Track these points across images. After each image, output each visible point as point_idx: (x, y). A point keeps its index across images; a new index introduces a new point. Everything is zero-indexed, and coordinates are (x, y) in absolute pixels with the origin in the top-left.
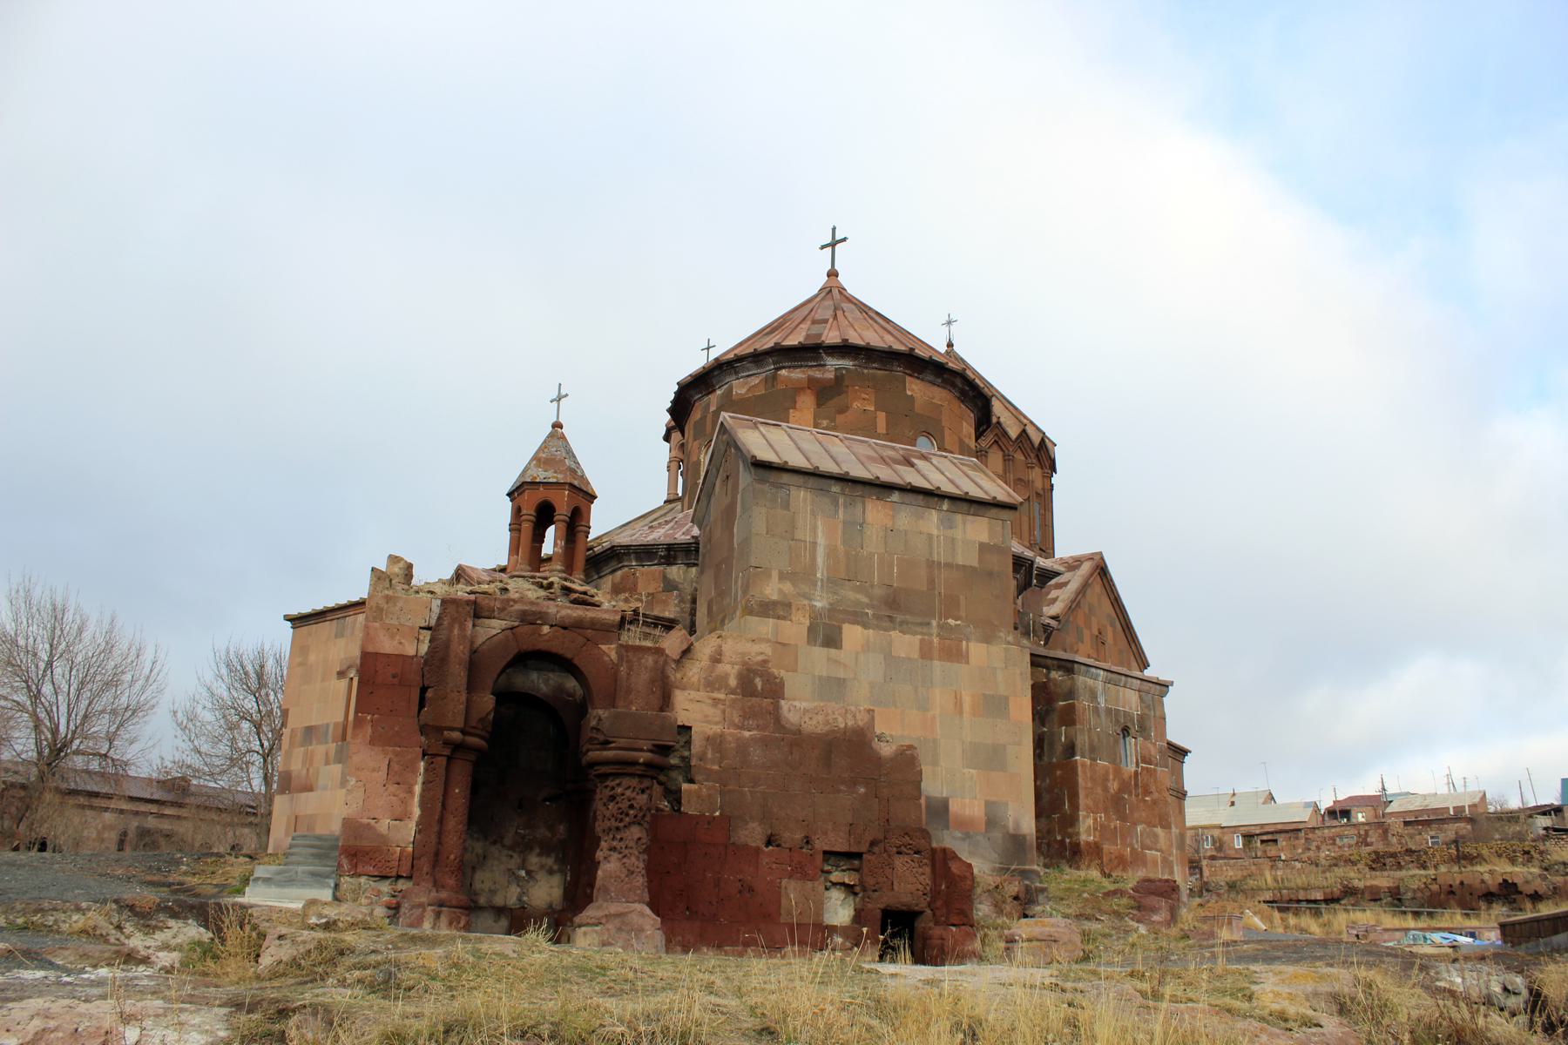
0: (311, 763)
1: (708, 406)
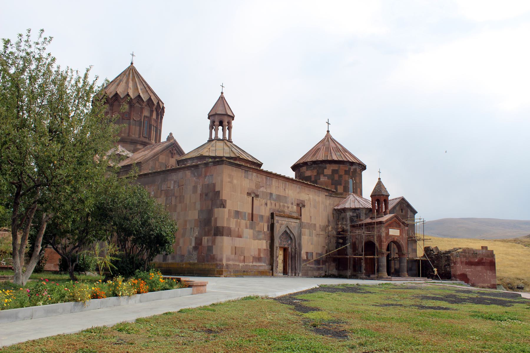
0: (240, 226)
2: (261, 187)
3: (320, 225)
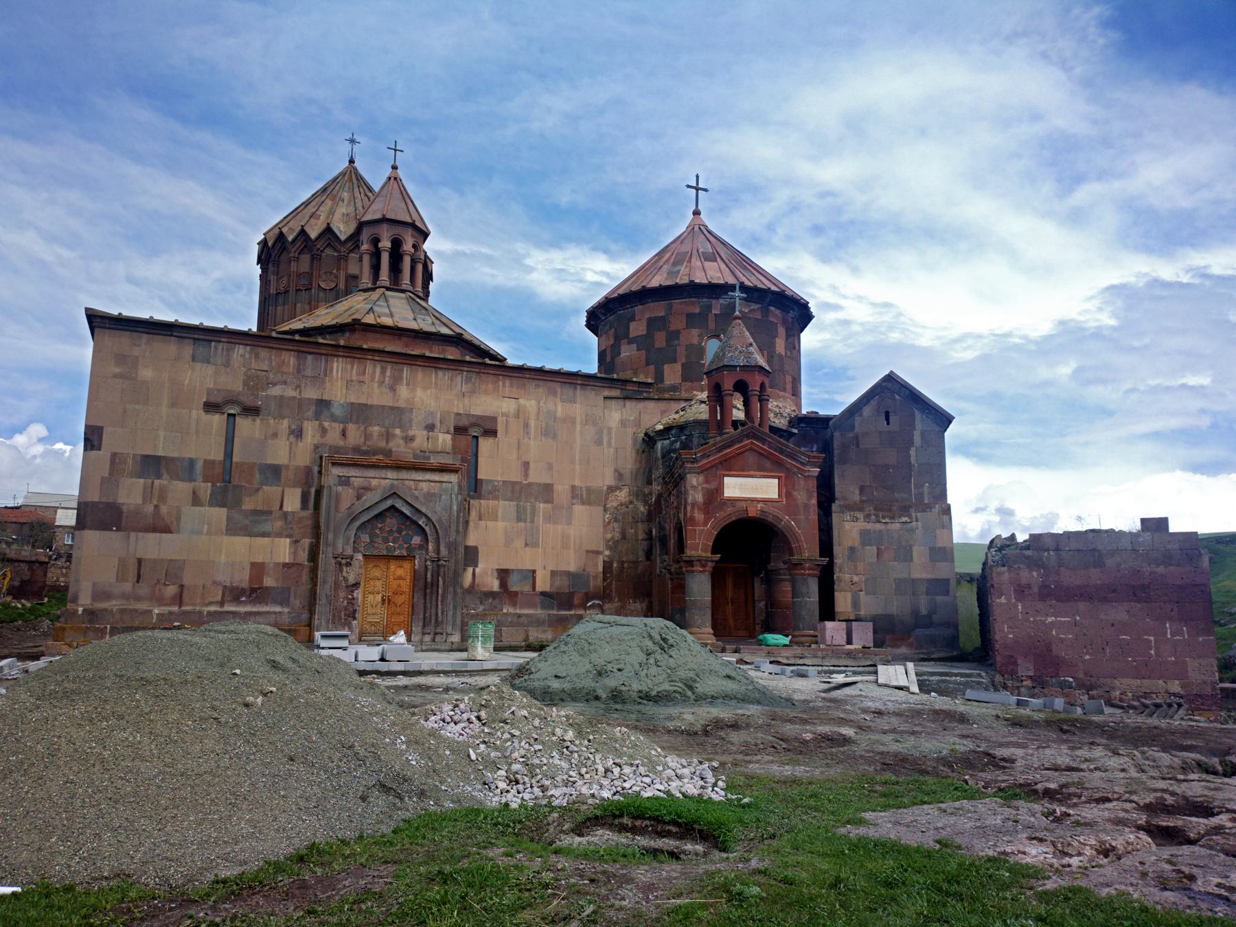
2: (274, 385)
3: (573, 487)
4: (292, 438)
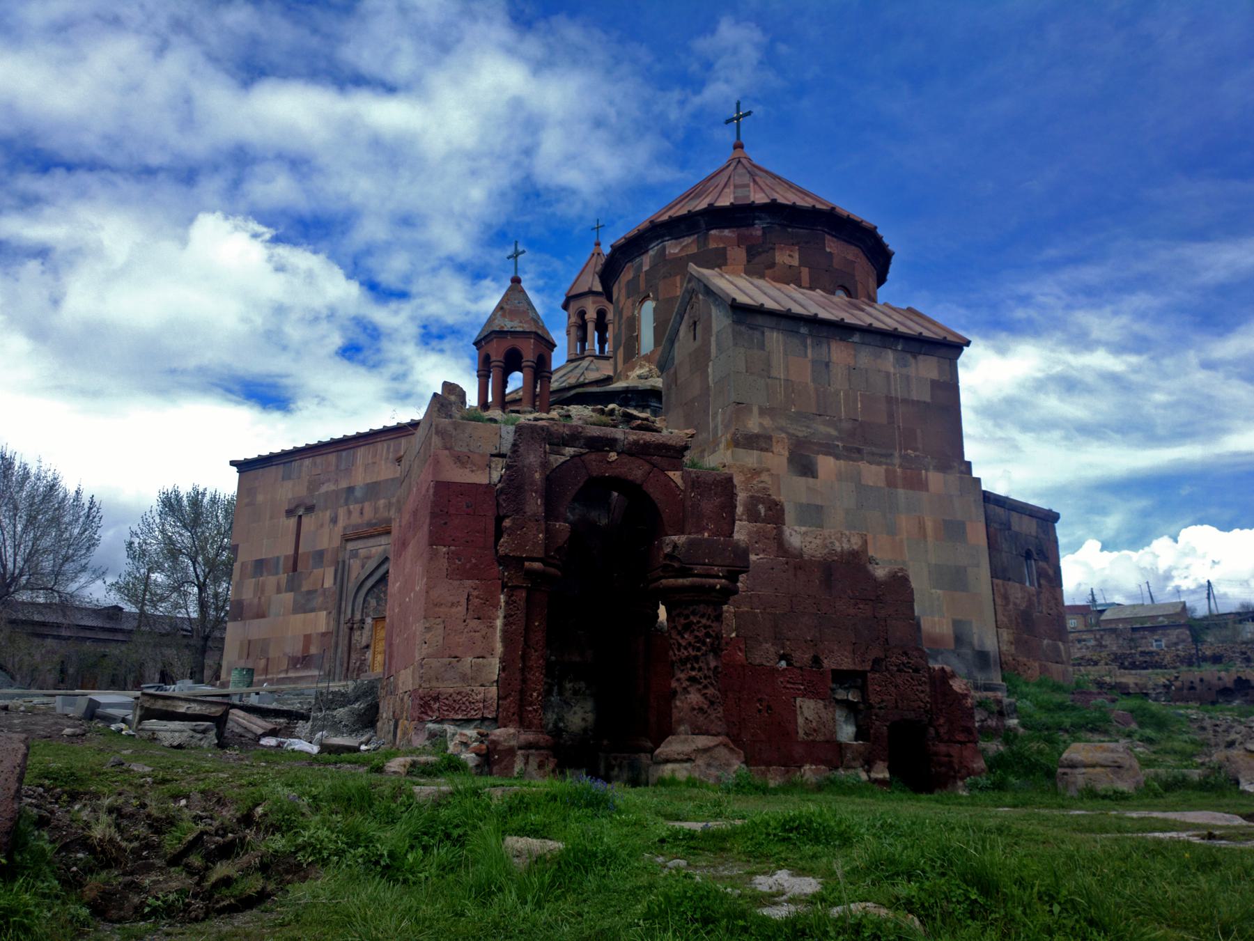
0: (263, 591)
1: (641, 265)
4: (331, 526)
